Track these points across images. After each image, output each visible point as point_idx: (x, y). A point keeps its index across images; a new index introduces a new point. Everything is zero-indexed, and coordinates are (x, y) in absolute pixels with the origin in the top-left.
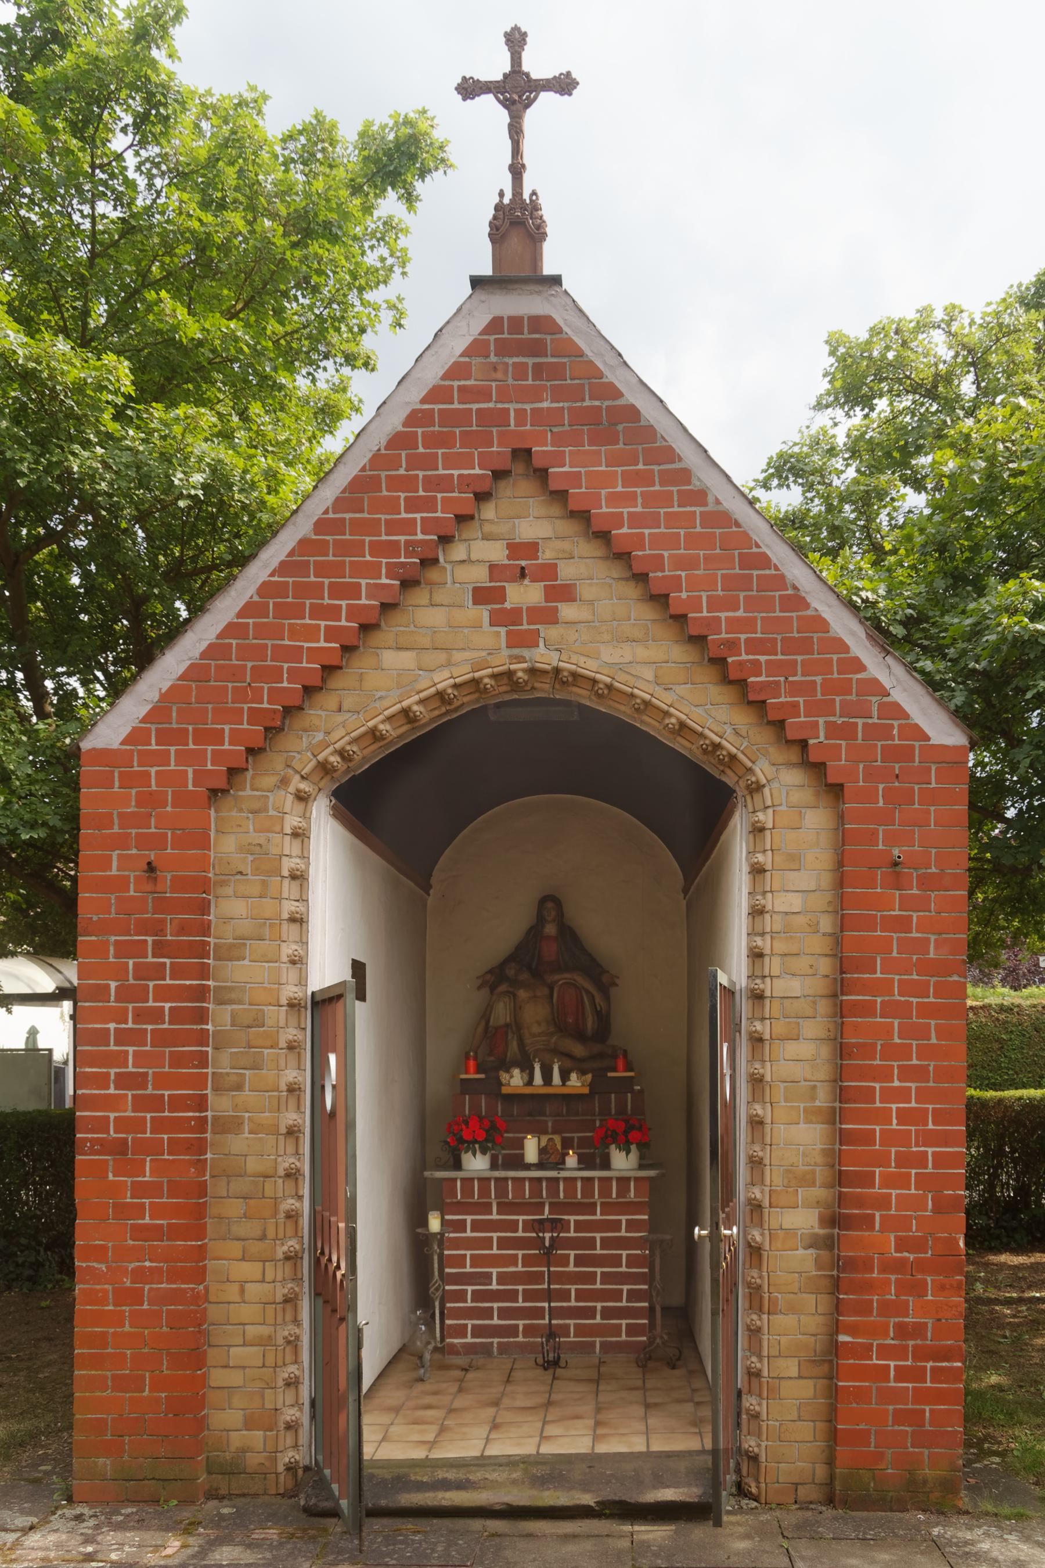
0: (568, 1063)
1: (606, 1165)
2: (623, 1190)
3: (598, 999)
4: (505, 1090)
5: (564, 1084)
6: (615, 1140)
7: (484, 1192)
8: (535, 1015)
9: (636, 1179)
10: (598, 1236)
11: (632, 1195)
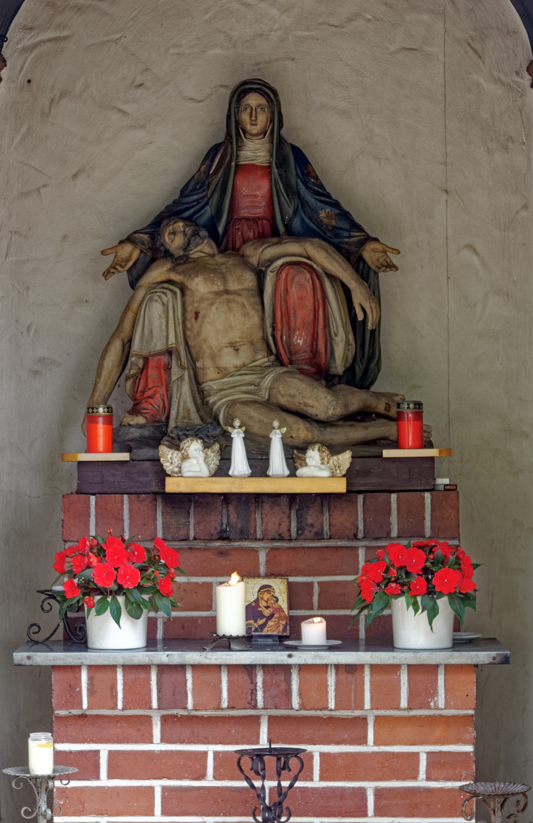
0: (302, 431)
1: (383, 636)
2: (421, 695)
3: (360, 296)
4: (172, 486)
5: (293, 474)
6: (404, 588)
7: (137, 695)
8: (225, 325)
9: (449, 668)
10: (370, 786)
11: (441, 703)
